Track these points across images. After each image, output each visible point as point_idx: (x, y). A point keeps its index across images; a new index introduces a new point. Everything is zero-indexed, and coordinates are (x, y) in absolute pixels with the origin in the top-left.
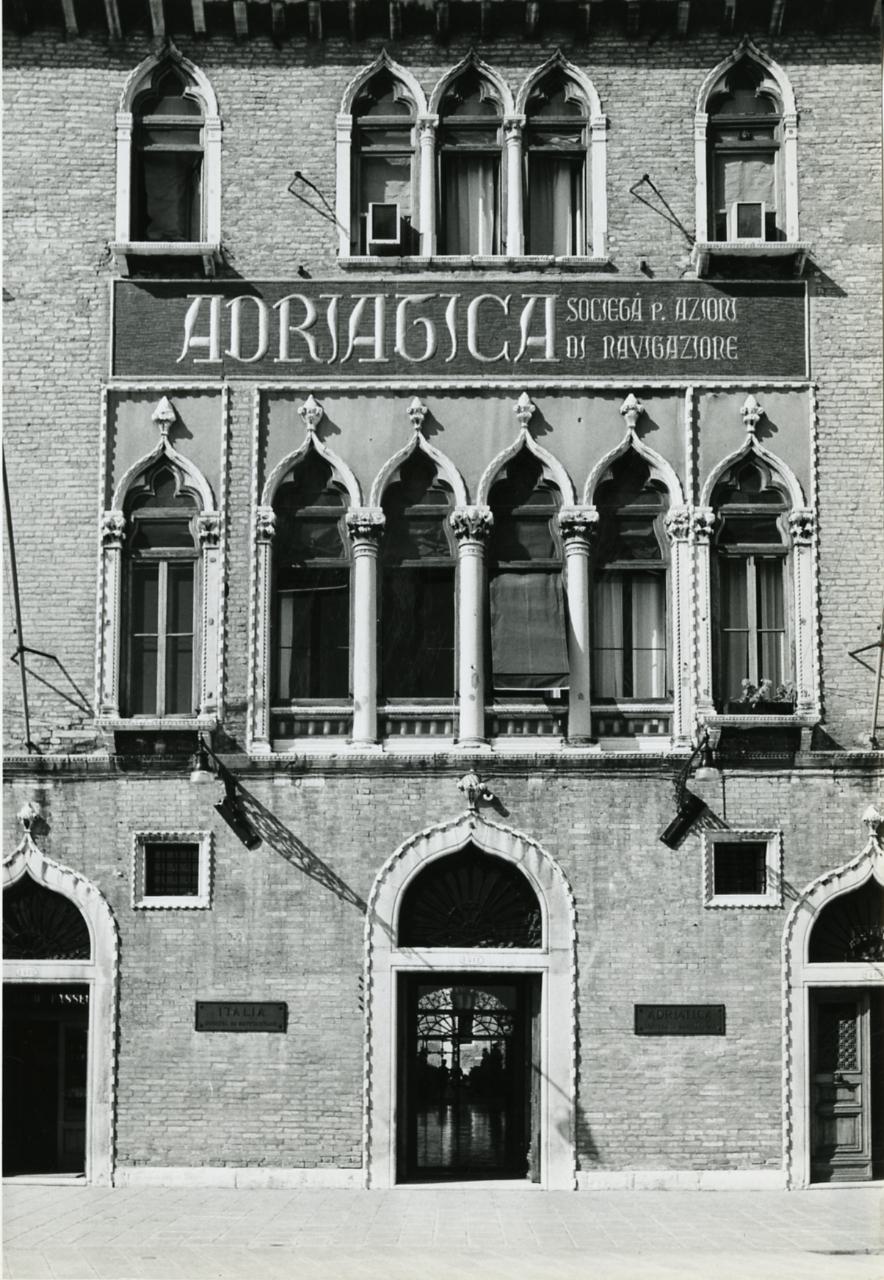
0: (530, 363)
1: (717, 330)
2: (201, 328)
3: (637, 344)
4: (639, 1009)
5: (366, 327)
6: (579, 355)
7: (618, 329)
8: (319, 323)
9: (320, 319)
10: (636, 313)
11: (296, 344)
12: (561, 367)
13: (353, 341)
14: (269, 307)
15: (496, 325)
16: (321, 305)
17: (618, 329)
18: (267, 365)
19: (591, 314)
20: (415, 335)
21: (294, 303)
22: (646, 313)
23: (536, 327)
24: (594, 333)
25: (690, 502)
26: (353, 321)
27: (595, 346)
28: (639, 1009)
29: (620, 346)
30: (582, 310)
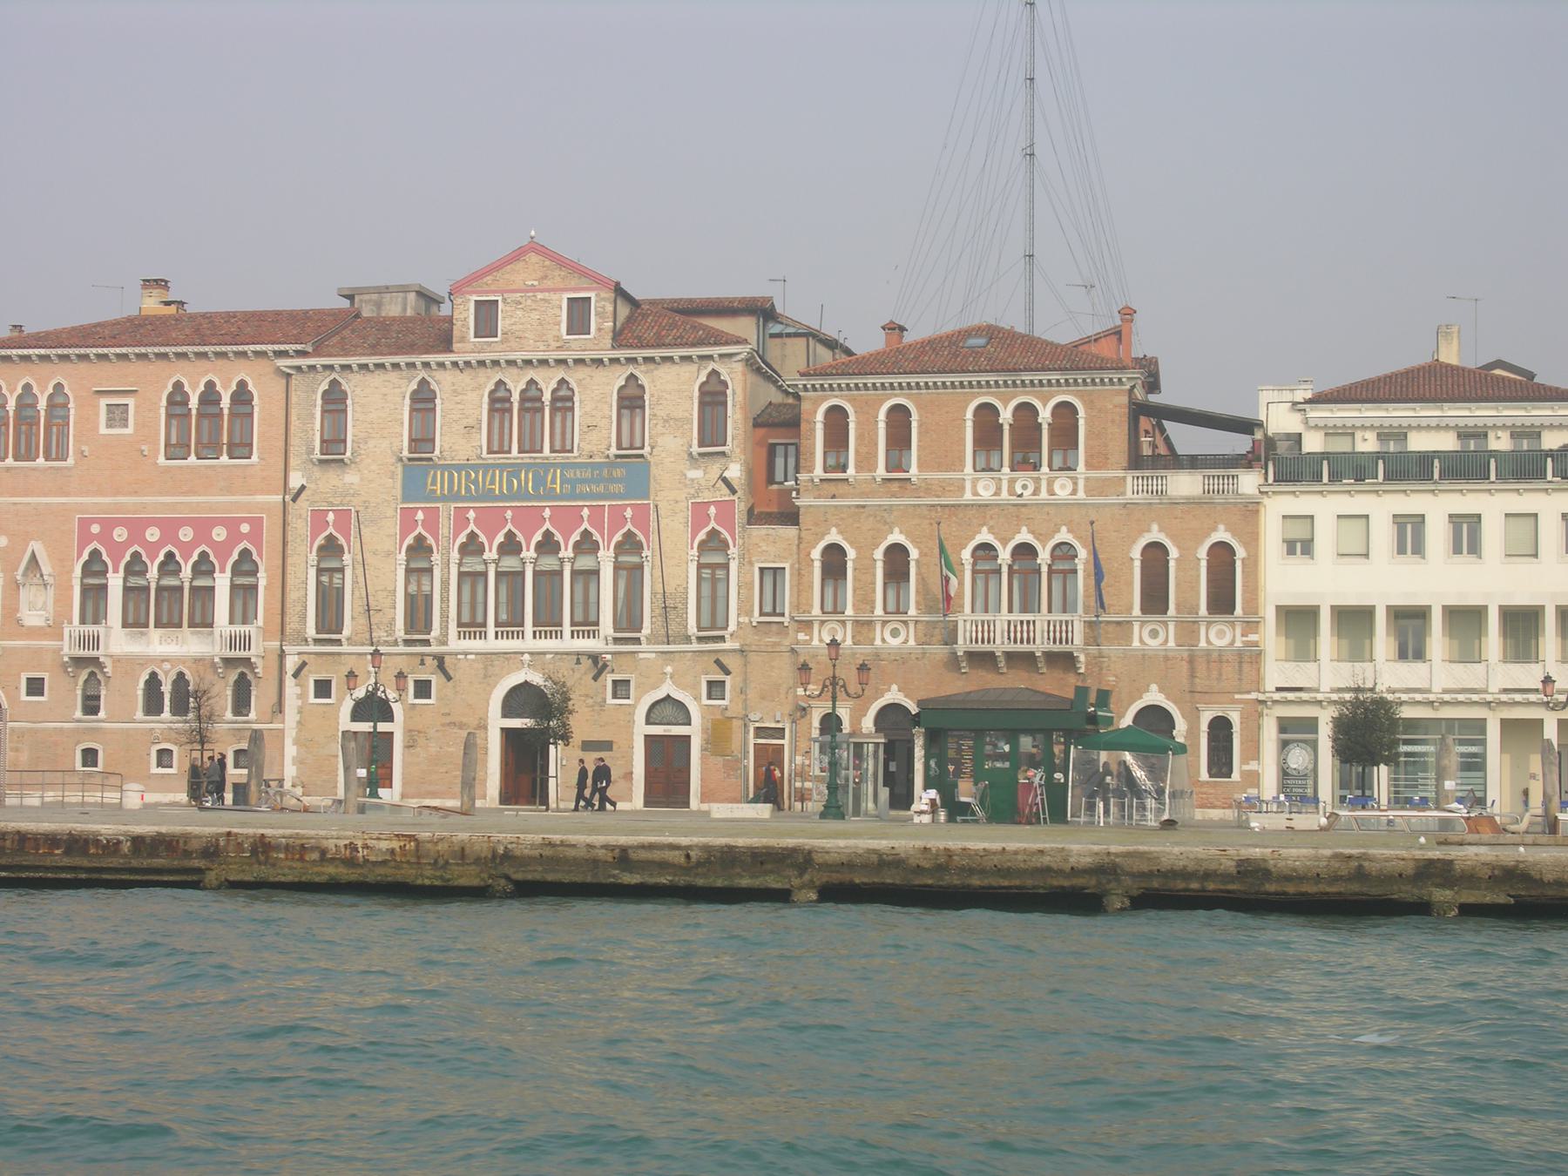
0: (551, 495)
1: (618, 481)
2: (434, 483)
4: (583, 742)
5: (492, 483)
8: (476, 482)
11: (468, 489)
12: (561, 497)
15: (539, 481)
18: (456, 497)
20: (510, 483)
21: (467, 472)
22: (593, 475)
23: (554, 481)
24: (574, 482)
26: (489, 478)
27: (574, 488)
28: (583, 742)
30: (569, 474)
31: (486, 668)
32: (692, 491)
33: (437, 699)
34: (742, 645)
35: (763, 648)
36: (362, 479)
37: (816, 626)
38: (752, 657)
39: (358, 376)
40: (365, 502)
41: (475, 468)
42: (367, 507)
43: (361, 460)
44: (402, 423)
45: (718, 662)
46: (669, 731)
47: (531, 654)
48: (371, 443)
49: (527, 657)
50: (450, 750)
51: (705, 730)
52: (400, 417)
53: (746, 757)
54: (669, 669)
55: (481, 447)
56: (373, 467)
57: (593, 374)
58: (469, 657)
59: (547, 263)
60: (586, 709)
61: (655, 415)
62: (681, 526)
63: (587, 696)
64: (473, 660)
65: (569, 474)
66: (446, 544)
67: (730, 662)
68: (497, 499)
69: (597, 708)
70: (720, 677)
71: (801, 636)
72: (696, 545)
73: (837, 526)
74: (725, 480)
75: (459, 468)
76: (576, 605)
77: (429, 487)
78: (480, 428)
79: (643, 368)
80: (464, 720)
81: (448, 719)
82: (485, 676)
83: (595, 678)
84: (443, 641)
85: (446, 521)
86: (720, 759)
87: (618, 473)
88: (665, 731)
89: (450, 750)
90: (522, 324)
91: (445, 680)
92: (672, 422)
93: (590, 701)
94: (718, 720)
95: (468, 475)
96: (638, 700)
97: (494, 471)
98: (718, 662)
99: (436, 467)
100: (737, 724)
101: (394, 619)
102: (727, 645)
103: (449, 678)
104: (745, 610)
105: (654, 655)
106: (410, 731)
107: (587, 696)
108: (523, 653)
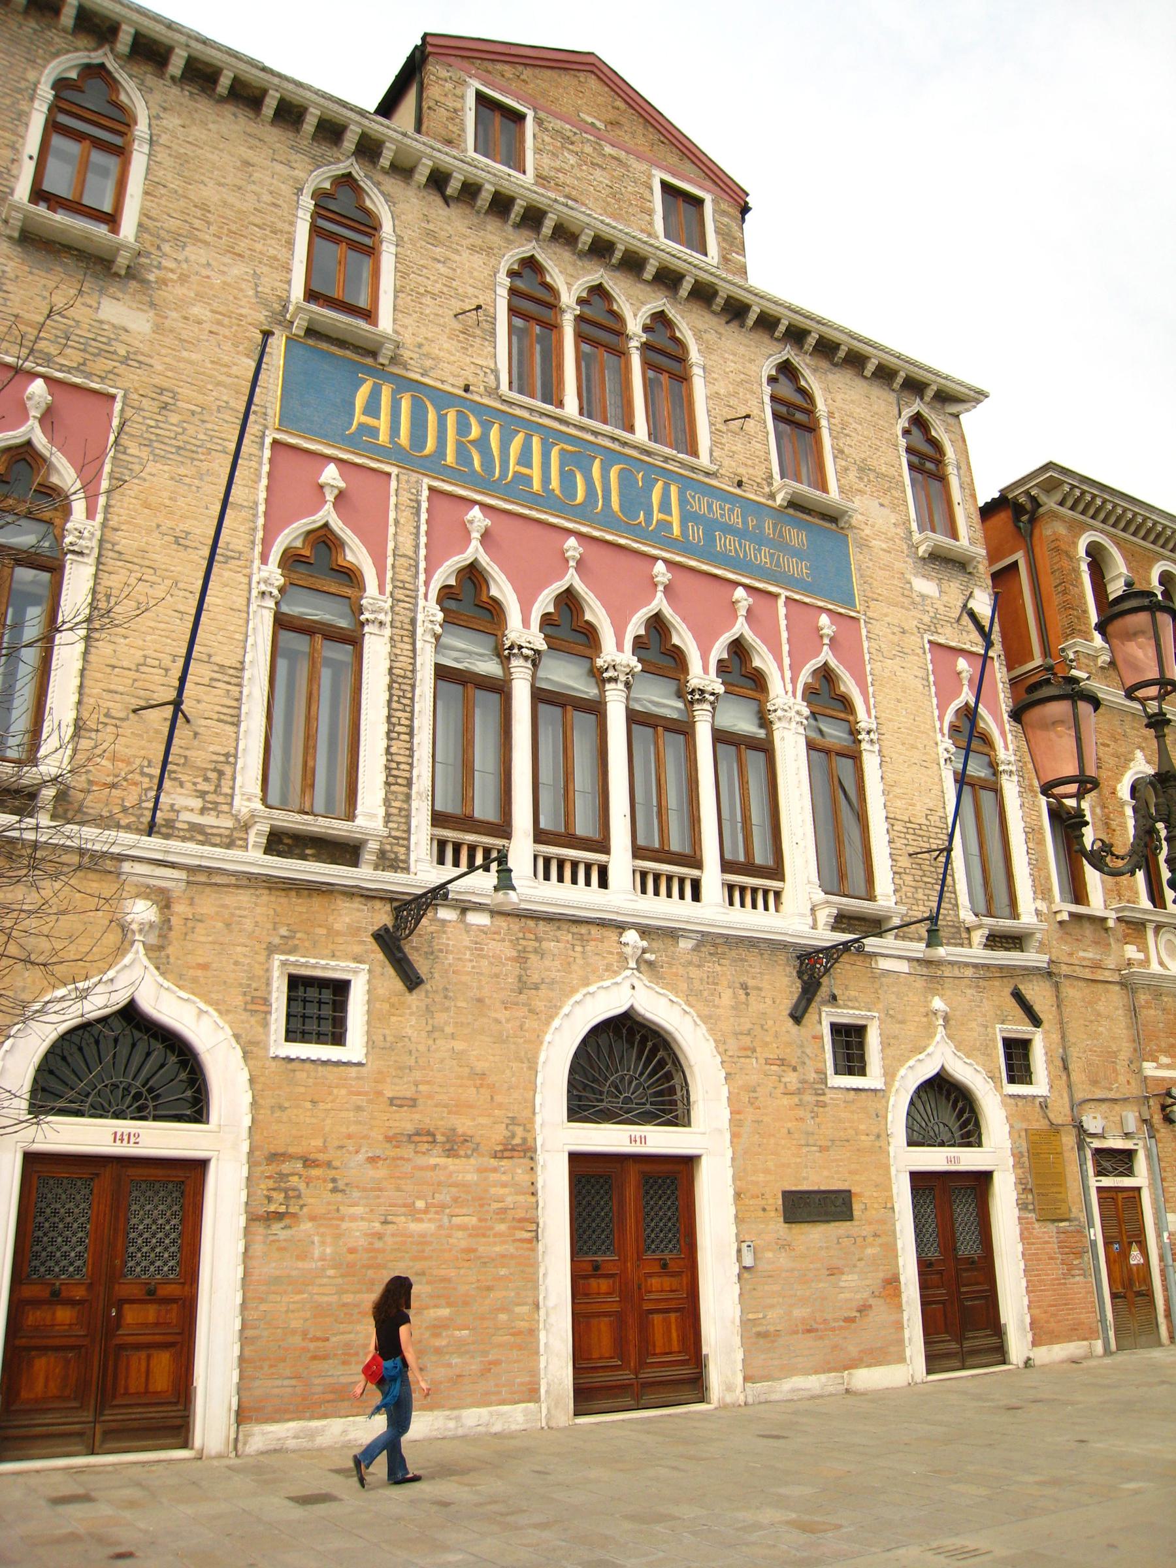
0: (661, 535)
2: (372, 408)
3: (740, 545)
4: (787, 1195)
6: (699, 541)
7: (728, 529)
8: (482, 444)
9: (485, 437)
10: (736, 520)
13: (513, 467)
14: (438, 412)
15: (635, 499)
16: (486, 426)
17: (728, 529)
19: (704, 510)
20: (567, 479)
22: (745, 522)
23: (665, 507)
24: (711, 526)
25: (790, 693)
28: (787, 1195)
29: (725, 543)
30: (699, 505)
31: (521, 959)
32: (926, 619)
33: (371, 1044)
34: (1051, 962)
35: (1080, 972)
36: (158, 328)
37: (1150, 934)
38: (1071, 992)
39: (175, 90)
40: (162, 390)
41: (487, 415)
42: (165, 406)
43: (165, 282)
44: (290, 244)
45: (1018, 996)
46: (957, 1160)
47: (645, 931)
48: (195, 254)
49: (631, 936)
50: (414, 1227)
51: (1017, 1155)
52: (286, 227)
53: (1091, 1224)
54: (937, 1003)
55: (495, 372)
56: (197, 310)
57: (721, 330)
58: (474, 918)
59: (619, 103)
60: (786, 1101)
61: (842, 452)
62: (919, 684)
63: (782, 1062)
64: (482, 930)
65: (699, 505)
66: (405, 576)
67: (1038, 994)
68: (535, 501)
69: (809, 1098)
70: (1021, 1029)
71: (1131, 951)
72: (946, 731)
73: (1142, 749)
74: (972, 615)
75: (443, 399)
76: (723, 822)
77: (359, 418)
78: (493, 333)
79: (808, 359)
80: (463, 1125)
81: (406, 1122)
82: (523, 985)
83: (797, 1017)
84: (390, 861)
85: (406, 515)
86: (1051, 1228)
87: (796, 537)
88: (949, 1160)
89: (414, 1227)
90: (578, 179)
91: (399, 985)
92: (872, 476)
93: (791, 1078)
94: (1038, 1133)
95: (463, 427)
96: (889, 1074)
97: (529, 437)
98: (1018, 996)
99: (380, 373)
100: (1069, 1140)
101: (231, 758)
102: (1031, 957)
103: (412, 980)
104: (1042, 891)
105: (903, 967)
106: (274, 1157)
107: (782, 1062)
108: (621, 927)
